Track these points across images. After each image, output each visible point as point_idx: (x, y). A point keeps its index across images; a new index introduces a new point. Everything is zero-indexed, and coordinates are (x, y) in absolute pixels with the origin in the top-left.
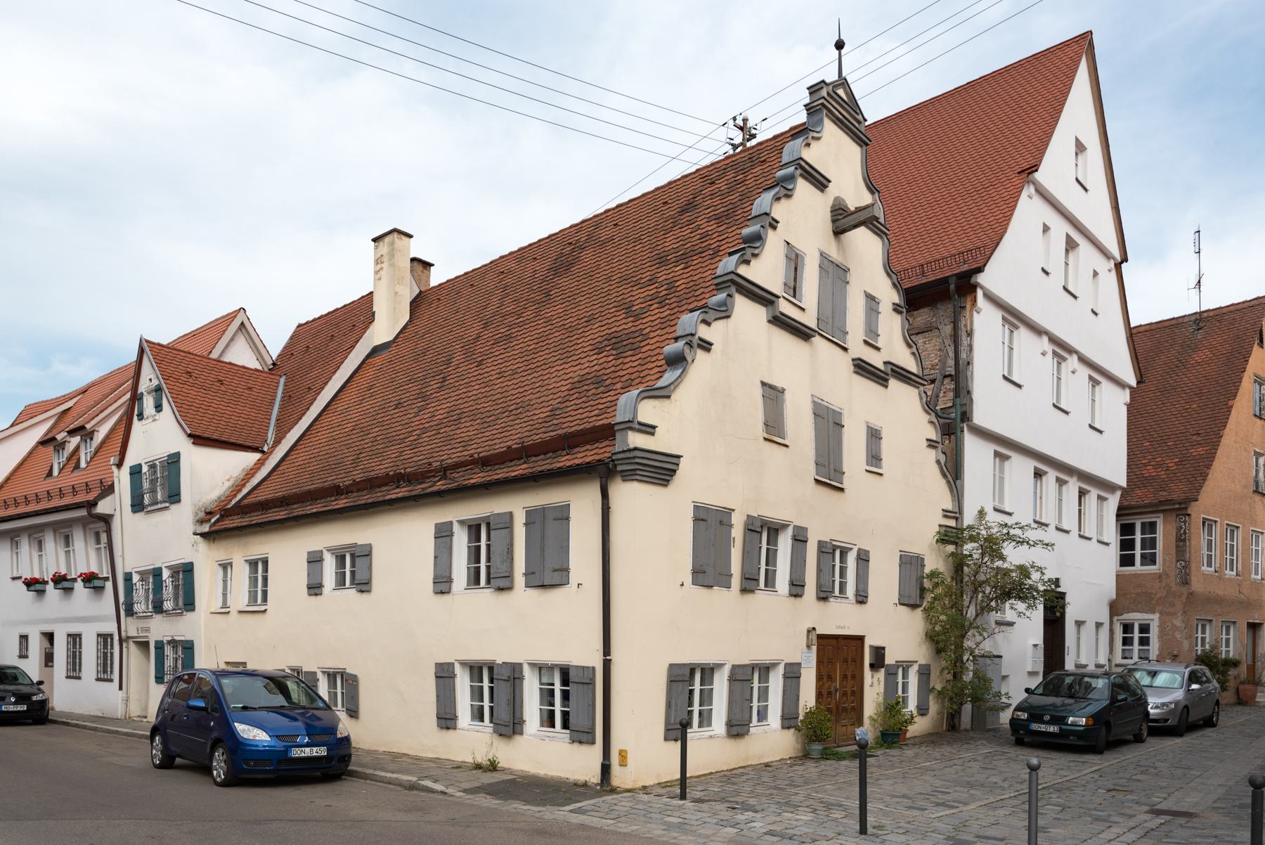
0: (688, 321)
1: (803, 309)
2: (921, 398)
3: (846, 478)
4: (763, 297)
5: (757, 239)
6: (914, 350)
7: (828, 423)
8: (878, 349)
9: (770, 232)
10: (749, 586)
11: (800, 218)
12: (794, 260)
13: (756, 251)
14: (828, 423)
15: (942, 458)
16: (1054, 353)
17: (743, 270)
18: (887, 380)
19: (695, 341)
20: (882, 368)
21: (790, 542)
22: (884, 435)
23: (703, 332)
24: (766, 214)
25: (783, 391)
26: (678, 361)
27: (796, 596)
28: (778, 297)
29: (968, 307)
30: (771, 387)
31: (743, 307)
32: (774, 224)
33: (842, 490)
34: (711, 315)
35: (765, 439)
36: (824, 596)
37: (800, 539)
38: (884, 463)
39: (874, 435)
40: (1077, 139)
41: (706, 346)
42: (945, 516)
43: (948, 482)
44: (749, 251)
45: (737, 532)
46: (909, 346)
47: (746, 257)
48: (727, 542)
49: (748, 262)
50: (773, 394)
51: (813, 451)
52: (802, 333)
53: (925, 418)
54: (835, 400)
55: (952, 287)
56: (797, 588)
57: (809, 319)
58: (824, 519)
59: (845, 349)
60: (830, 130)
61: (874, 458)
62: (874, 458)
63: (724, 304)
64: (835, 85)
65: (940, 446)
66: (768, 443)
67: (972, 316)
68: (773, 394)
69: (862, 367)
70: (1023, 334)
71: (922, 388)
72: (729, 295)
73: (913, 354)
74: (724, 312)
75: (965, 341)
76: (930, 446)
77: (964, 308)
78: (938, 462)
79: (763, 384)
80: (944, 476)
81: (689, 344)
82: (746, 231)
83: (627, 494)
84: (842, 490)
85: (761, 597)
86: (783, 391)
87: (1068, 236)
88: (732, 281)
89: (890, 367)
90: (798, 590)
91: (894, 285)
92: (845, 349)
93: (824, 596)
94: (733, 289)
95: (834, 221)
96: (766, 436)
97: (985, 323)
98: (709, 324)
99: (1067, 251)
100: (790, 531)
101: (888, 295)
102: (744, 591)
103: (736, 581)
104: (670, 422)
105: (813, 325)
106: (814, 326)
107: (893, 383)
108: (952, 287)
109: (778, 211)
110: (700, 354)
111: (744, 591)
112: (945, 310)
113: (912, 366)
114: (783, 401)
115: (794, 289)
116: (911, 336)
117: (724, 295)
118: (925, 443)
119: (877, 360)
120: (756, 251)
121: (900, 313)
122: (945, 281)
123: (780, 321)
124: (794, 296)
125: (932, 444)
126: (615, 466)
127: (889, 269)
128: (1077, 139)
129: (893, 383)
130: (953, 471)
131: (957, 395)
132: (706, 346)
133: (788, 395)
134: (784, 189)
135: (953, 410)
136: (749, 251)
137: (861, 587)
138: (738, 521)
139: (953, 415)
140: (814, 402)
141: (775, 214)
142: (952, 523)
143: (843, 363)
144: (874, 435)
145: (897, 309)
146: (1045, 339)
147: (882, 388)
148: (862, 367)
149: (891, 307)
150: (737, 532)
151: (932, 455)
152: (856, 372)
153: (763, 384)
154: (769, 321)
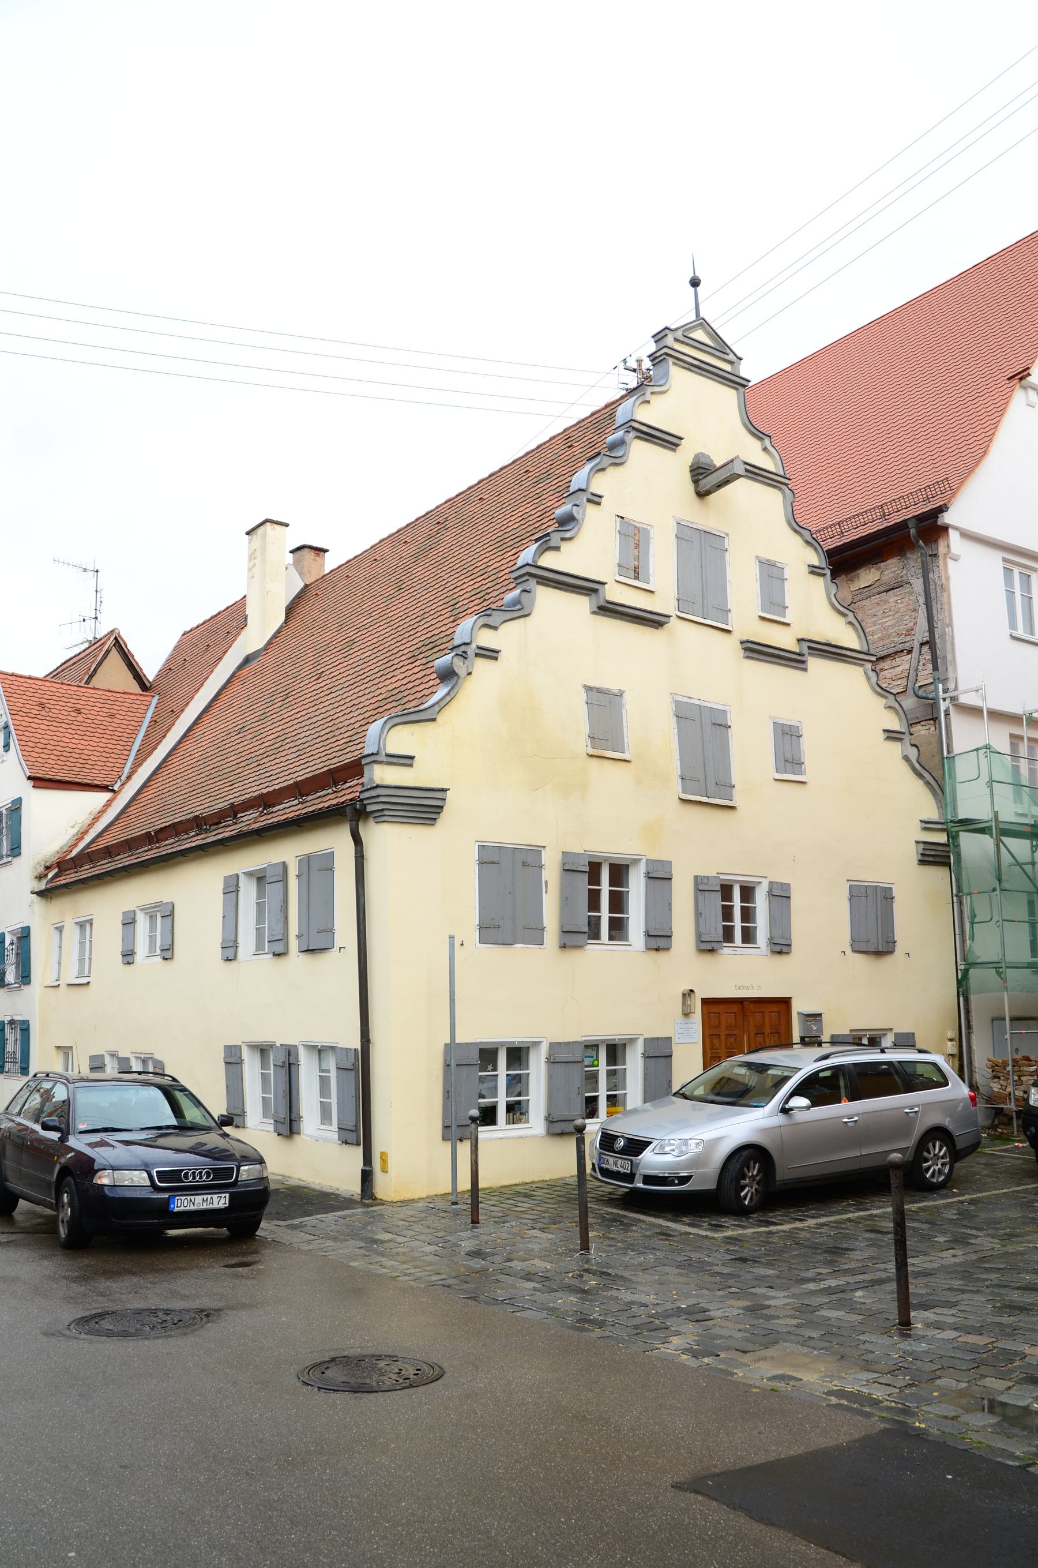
3: (736, 793)
9: (590, 508)
11: (643, 488)
12: (633, 537)
13: (568, 535)
17: (549, 560)
19: (471, 650)
21: (643, 881)
23: (486, 639)
25: (621, 694)
26: (448, 675)
30: (599, 691)
32: (595, 500)
34: (496, 618)
36: (707, 948)
37: (660, 878)
41: (490, 654)
47: (552, 544)
50: (604, 703)
51: (678, 763)
54: (708, 693)
63: (517, 601)
64: (687, 328)
66: (595, 761)
67: (945, 563)
68: (604, 703)
69: (756, 651)
74: (519, 611)
79: (588, 689)
81: (464, 656)
84: (732, 808)
86: (621, 694)
89: (805, 645)
93: (707, 948)
94: (532, 583)
95: (696, 482)
96: (592, 751)
98: (495, 628)
100: (642, 868)
110: (481, 666)
114: (621, 706)
115: (635, 570)
117: (517, 592)
120: (568, 535)
123: (609, 610)
124: (637, 578)
127: (796, 527)
132: (490, 654)
133: (627, 698)
134: (613, 454)
154: (594, 613)
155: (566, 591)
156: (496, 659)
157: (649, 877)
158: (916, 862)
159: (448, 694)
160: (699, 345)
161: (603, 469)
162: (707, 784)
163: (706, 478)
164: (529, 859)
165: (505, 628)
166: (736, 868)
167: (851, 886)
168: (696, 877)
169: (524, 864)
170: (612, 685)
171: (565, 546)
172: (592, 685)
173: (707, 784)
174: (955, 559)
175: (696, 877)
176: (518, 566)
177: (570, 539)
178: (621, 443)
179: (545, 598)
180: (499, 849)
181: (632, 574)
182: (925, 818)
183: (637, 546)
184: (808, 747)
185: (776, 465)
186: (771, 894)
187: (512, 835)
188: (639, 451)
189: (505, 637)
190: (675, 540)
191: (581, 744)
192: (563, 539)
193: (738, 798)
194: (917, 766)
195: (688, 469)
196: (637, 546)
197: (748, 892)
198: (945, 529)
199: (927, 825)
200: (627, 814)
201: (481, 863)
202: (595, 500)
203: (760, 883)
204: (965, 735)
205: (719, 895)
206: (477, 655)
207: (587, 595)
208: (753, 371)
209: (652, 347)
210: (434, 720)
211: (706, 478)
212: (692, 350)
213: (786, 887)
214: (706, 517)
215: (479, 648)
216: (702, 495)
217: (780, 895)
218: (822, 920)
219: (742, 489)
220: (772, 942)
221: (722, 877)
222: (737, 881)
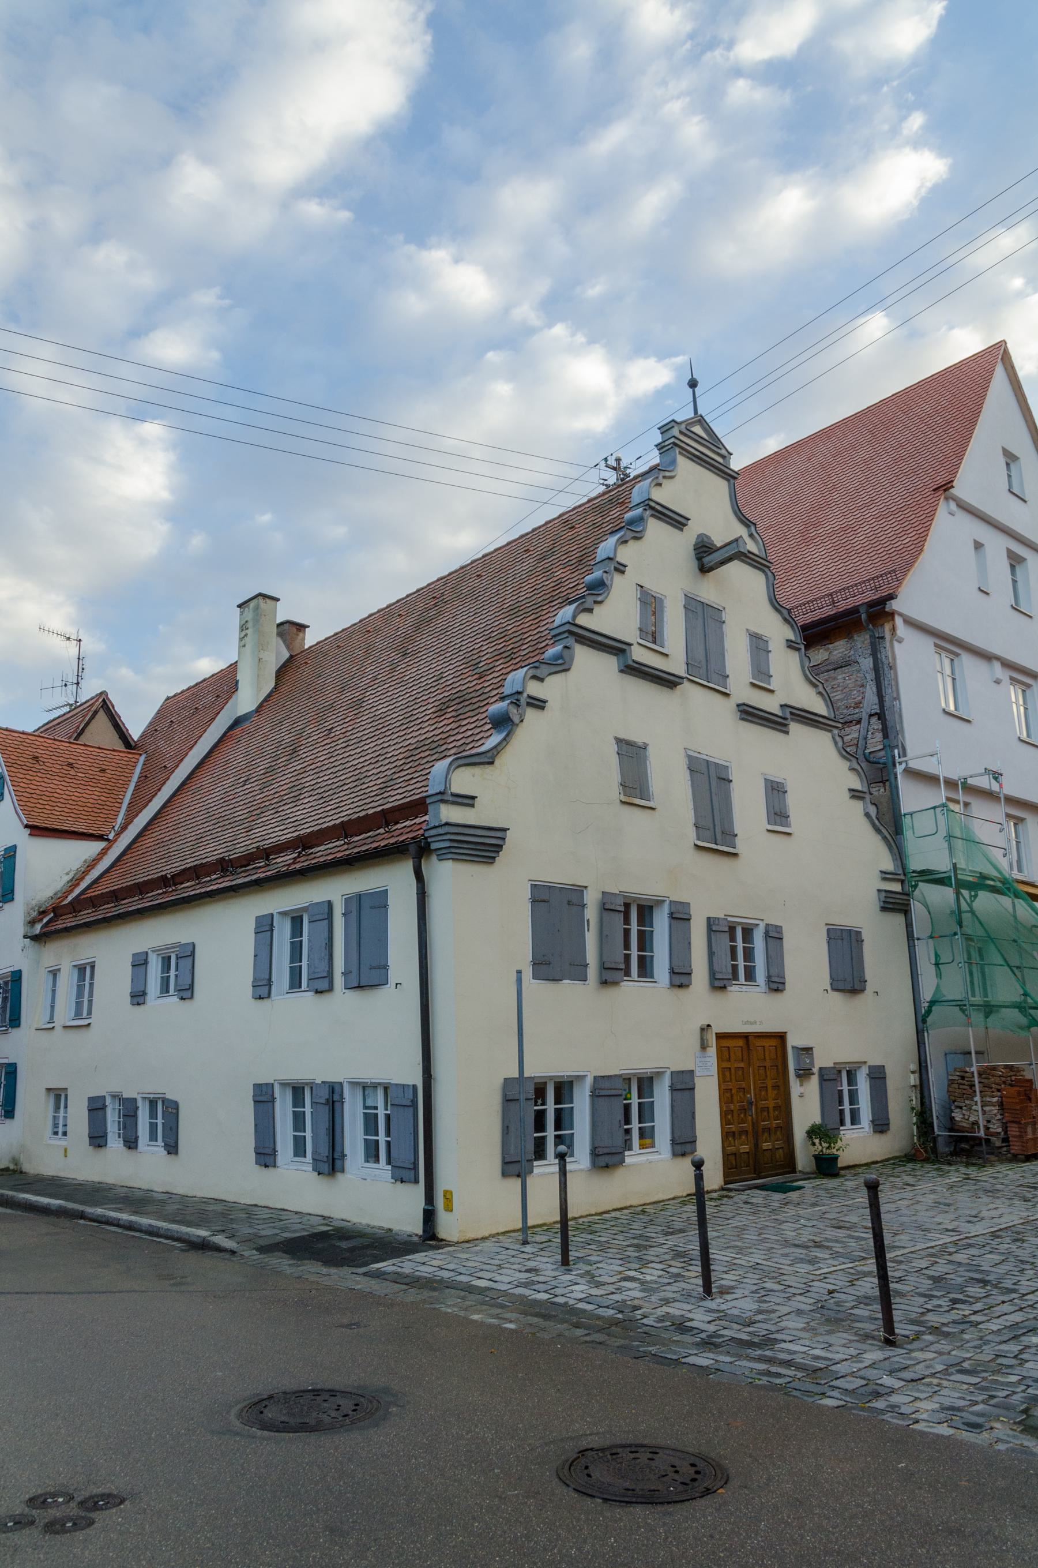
0: (515, 679)
1: (667, 655)
2: (836, 743)
3: (738, 841)
4: (615, 648)
5: (599, 587)
6: (821, 689)
7: (710, 781)
8: (772, 691)
9: (617, 578)
10: (611, 975)
11: (655, 560)
12: (650, 604)
13: (599, 599)
14: (710, 781)
15: (873, 811)
16: (1012, 678)
17: (583, 620)
18: (786, 725)
19: (523, 699)
20: (777, 711)
22: (788, 788)
23: (534, 689)
24: (609, 559)
25: (645, 747)
26: (503, 723)
27: (681, 986)
28: (630, 645)
29: (888, 635)
30: (629, 743)
31: (583, 657)
32: (621, 569)
33: (735, 855)
35: (623, 803)
36: (719, 984)
37: (680, 917)
38: (792, 819)
39: (775, 790)
40: (1004, 450)
41: (538, 704)
42: (884, 879)
43: (884, 838)
44: (590, 600)
45: (591, 914)
46: (815, 686)
47: (586, 606)
48: (580, 925)
49: (590, 611)
50: (631, 754)
52: (667, 681)
53: (843, 765)
54: (715, 752)
55: (864, 616)
56: (680, 978)
57: (676, 665)
58: (711, 892)
59: (727, 695)
60: (684, 465)
61: (778, 815)
62: (778, 815)
63: (559, 656)
65: (868, 796)
66: (627, 808)
67: (892, 647)
68: (631, 754)
70: (967, 660)
71: (836, 732)
72: (566, 647)
73: (820, 693)
74: (562, 665)
75: (889, 675)
76: (853, 797)
77: (883, 638)
78: (867, 815)
79: (619, 741)
80: (878, 831)
81: (517, 704)
82: (588, 578)
83: (447, 876)
84: (735, 855)
85: (631, 988)
86: (645, 747)
87: (1009, 551)
88: (570, 632)
90: (683, 980)
91: (785, 620)
92: (727, 695)
93: (719, 984)
95: (699, 559)
97: (910, 656)
98: (542, 680)
99: (1013, 567)
100: (666, 909)
101: (778, 633)
102: (604, 983)
103: (592, 971)
104: (492, 794)
105: (680, 670)
106: (683, 674)
107: (794, 727)
108: (864, 616)
109: (624, 555)
110: (531, 714)
111: (604, 983)
112: (862, 641)
113: (819, 707)
115: (652, 635)
116: (814, 675)
117: (559, 648)
118: (847, 795)
119: (770, 704)
120: (599, 599)
121: (798, 649)
122: (855, 610)
123: (636, 670)
124: (654, 642)
125: (855, 794)
126: (429, 844)
128: (1004, 450)
129: (794, 727)
130: (890, 824)
131: (886, 736)
132: (538, 704)
133: (651, 751)
134: (633, 530)
135: (882, 753)
136: (590, 600)
137: (773, 972)
138: (592, 899)
139: (883, 760)
140: (689, 756)
141: (619, 559)
142: (896, 887)
143: (726, 709)
144: (775, 790)
145: (791, 645)
146: (997, 665)
147: (781, 735)
148: (749, 713)
149: (784, 644)
150: (591, 914)
151: (858, 806)
152: (743, 719)
153: (619, 741)
154: (621, 671)
155: (599, 650)
156: (543, 708)
157: (672, 916)
158: (878, 908)
159: (504, 739)
160: (697, 439)
161: (626, 542)
162: (716, 836)
163: (707, 557)
164: (574, 896)
165: (551, 680)
166: (741, 911)
167: (828, 930)
168: (709, 919)
169: (569, 903)
170: (639, 739)
171: (597, 609)
172: (622, 736)
173: (716, 836)
174: (900, 641)
175: (709, 919)
176: (556, 624)
177: (601, 602)
178: (640, 519)
179: (582, 655)
180: (549, 888)
181: (650, 639)
182: (884, 869)
183: (654, 613)
184: (793, 802)
185: (759, 550)
186: (767, 935)
187: (559, 874)
188: (654, 528)
189: (548, 689)
190: (683, 610)
191: (614, 792)
192: (596, 602)
193: (741, 846)
194: (876, 822)
195: (692, 548)
196: (654, 613)
197: (748, 933)
198: (892, 615)
199: (885, 876)
200: (651, 855)
201: (534, 901)
202: (621, 569)
203: (757, 925)
204: (912, 798)
205: (727, 935)
206: (529, 704)
207: (615, 655)
208: (737, 464)
209: (659, 439)
210: (492, 763)
211: (707, 557)
212: (690, 442)
213: (779, 929)
214: (708, 590)
215: (529, 697)
216: (704, 569)
217: (774, 936)
218: (807, 960)
219: (736, 570)
220: (769, 980)
221: (729, 919)
222: (739, 923)
